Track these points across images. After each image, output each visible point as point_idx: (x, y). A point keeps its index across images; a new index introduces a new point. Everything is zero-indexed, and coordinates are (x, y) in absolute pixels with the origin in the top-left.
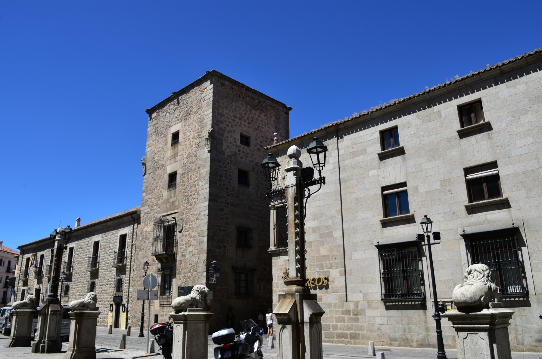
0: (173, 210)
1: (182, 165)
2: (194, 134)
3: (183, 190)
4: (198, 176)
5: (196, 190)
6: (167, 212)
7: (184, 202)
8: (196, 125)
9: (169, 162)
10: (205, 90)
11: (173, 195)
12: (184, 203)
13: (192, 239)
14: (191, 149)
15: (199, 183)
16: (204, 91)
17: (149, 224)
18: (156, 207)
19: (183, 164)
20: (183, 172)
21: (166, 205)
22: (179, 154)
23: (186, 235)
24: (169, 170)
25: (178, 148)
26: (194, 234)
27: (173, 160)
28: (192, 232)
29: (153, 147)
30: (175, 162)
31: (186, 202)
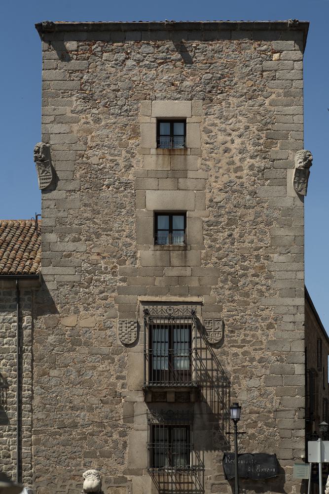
1: (207, 203)
2: (243, 143)
3: (214, 259)
4: (268, 240)
5: (262, 268)
7: (221, 285)
8: (251, 126)
9: (152, 182)
10: (276, 56)
11: (175, 261)
12: (222, 288)
13: (254, 363)
14: (239, 174)
15: (271, 255)
16: (271, 56)
17: (82, 313)
18: (109, 276)
19: (211, 201)
20: (212, 219)
21: (150, 279)
22: (191, 174)
23: (236, 355)
24: (155, 200)
25: (185, 159)
26: (262, 356)
27: (168, 183)
28: (255, 350)
29: (75, 127)
30: (178, 189)
31: (227, 286)
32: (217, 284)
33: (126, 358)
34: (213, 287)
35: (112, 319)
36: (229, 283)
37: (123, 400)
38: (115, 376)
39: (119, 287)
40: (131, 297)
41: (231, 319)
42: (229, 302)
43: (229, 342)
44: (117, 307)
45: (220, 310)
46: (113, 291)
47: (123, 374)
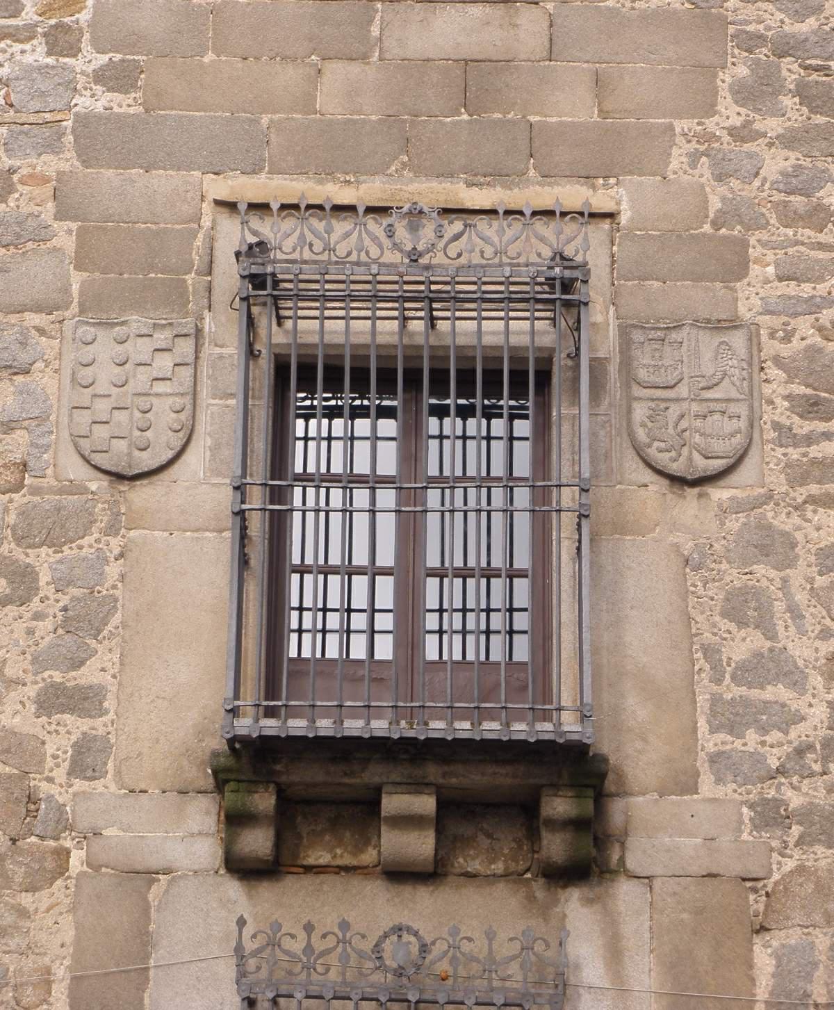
0: (499, 175)
6: (327, 172)
7: (730, 113)
12: (742, 134)
21: (288, 77)
31: (773, 126)
32: (710, 109)
33: (113, 570)
34: (680, 125)
35: (33, 319)
36: (788, 102)
37: (76, 861)
38: (31, 691)
39: (84, 121)
40: (164, 181)
41: (804, 326)
42: (789, 217)
43: (799, 474)
44: (65, 237)
45: (739, 269)
46: (52, 146)
47: (88, 675)
